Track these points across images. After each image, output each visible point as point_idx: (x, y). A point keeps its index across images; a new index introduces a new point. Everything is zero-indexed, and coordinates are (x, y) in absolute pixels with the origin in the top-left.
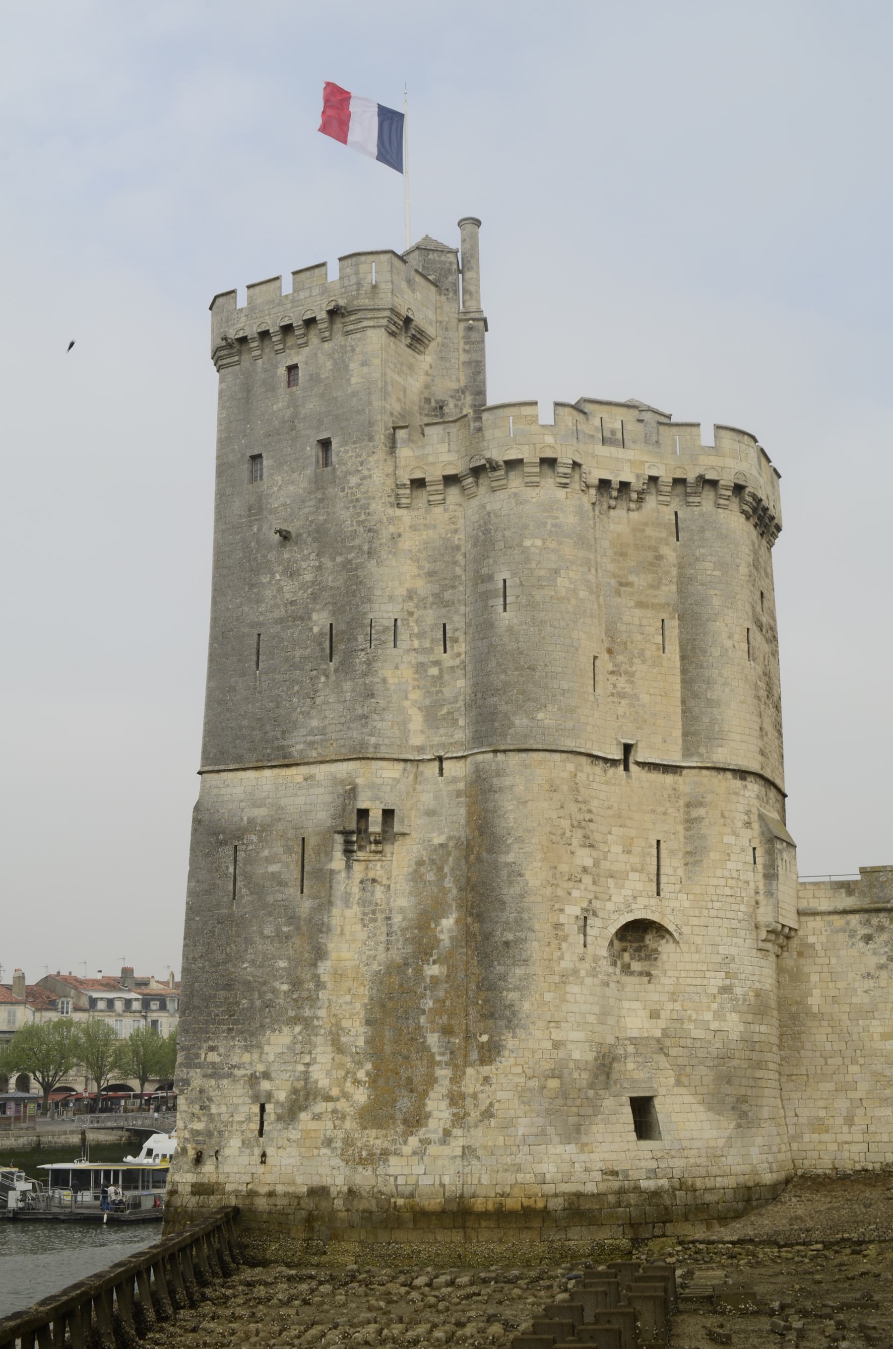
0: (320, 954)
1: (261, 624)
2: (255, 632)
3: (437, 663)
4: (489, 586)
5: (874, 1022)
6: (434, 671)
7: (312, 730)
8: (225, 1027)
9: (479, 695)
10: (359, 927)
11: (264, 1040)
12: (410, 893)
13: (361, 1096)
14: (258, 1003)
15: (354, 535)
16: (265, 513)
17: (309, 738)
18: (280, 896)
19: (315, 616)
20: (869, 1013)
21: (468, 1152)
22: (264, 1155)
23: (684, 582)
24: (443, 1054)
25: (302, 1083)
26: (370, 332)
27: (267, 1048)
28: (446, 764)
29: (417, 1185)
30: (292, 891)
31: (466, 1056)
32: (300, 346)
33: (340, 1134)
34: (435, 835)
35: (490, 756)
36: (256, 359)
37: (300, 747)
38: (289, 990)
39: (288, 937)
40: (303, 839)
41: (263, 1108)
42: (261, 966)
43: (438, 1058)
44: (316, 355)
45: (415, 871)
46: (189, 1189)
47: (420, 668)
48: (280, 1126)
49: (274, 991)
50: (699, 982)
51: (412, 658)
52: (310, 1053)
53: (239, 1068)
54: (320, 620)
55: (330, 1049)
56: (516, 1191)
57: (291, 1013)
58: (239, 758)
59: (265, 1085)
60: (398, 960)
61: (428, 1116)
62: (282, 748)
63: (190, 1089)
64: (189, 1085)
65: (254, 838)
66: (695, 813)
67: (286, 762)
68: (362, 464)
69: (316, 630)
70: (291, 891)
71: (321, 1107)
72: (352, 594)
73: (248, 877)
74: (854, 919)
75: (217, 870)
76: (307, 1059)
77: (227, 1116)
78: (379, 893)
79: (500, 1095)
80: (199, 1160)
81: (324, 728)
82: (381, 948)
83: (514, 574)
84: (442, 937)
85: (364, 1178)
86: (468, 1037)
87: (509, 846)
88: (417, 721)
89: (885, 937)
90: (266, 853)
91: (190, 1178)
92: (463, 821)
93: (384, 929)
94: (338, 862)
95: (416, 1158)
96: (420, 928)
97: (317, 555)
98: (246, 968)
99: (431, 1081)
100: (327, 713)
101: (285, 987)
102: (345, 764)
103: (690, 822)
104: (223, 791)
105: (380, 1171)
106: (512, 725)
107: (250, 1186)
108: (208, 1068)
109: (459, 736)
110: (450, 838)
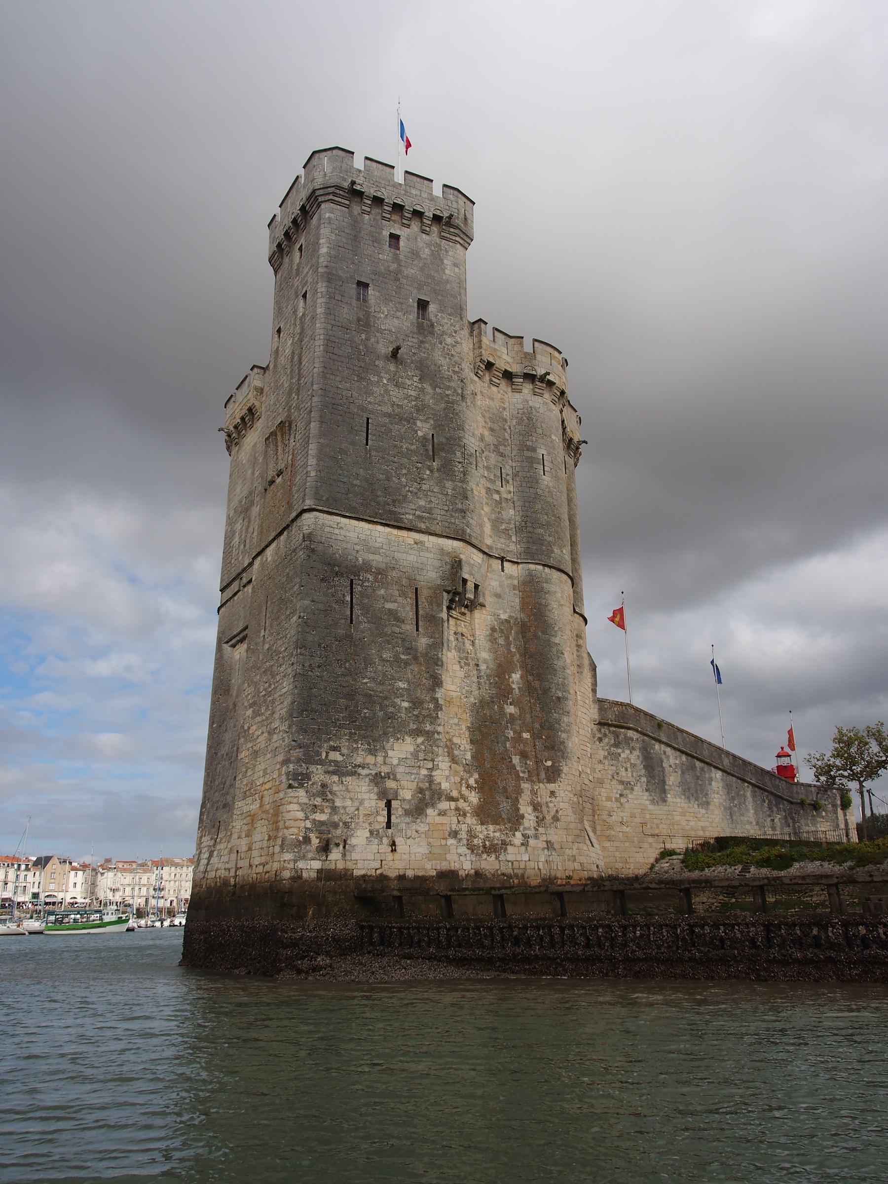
0: (436, 682)
1: (371, 412)
2: (365, 415)
3: (498, 492)
4: (533, 455)
5: (603, 790)
6: (496, 497)
7: (420, 507)
8: (347, 731)
9: (529, 524)
10: (457, 667)
11: (388, 746)
12: (490, 650)
13: (474, 798)
14: (381, 714)
15: (450, 379)
16: (373, 329)
17: (418, 513)
18: (397, 630)
19: (419, 423)
20: (601, 782)
21: (549, 845)
22: (393, 844)
24: (524, 772)
25: (427, 784)
26: (458, 246)
27: (390, 753)
28: (506, 564)
29: (525, 869)
30: (409, 627)
31: (538, 775)
32: (403, 225)
33: (464, 827)
34: (501, 612)
35: (541, 567)
36: (364, 212)
37: (411, 517)
38: (410, 707)
39: (407, 663)
40: (416, 589)
41: (388, 805)
42: (382, 683)
43: (521, 775)
44: (416, 239)
45: (491, 635)
46: (314, 875)
47: (488, 490)
48: (408, 820)
49: (394, 705)
50: (585, 748)
51: (483, 481)
52: (433, 760)
53: (363, 768)
54: (424, 428)
55: (447, 759)
56: (576, 877)
57: (413, 726)
58: (351, 509)
59: (391, 784)
60: (487, 697)
61: (523, 817)
62: (394, 513)
63: (310, 783)
64: (309, 779)
65: (371, 578)
66: (581, 642)
67: (399, 524)
68: (456, 332)
69: (420, 433)
70: (408, 627)
71: (444, 805)
72: (449, 421)
73: (366, 610)
75: (333, 596)
76: (430, 765)
77: (353, 809)
78: (468, 646)
79: (562, 805)
80: (325, 848)
81: (431, 509)
82: (475, 686)
83: (549, 454)
84: (514, 686)
85: (489, 864)
86: (538, 762)
87: (556, 632)
88: (488, 528)
89: (606, 740)
90: (382, 592)
91: (317, 865)
92: (518, 607)
93: (475, 672)
94: (444, 615)
95: (523, 848)
96: (499, 678)
97: (420, 379)
98: (367, 683)
99: (519, 791)
100: (433, 499)
101: (406, 704)
102: (450, 542)
104: (337, 531)
105: (502, 857)
106: (553, 552)
107: (378, 872)
108: (331, 765)
109: (512, 547)
110: (510, 617)
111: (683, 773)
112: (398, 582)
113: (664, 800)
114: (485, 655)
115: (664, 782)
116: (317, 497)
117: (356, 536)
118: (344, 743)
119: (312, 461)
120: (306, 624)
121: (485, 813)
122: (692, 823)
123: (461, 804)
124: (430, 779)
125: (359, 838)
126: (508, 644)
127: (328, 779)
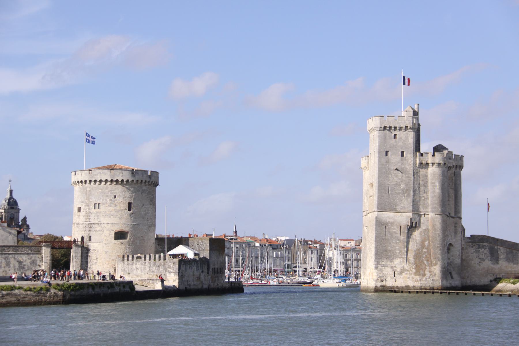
13: (414, 271)
21: (433, 280)
22: (396, 281)
23: (455, 184)
54: (403, 186)
58: (386, 210)
59: (395, 268)
71: (407, 272)
73: (389, 232)
74: (470, 244)
80: (382, 281)
91: (380, 284)
103: (455, 227)
111: (507, 254)
112: (396, 225)
113: (498, 263)
114: (418, 238)
115: (498, 258)
116: (378, 208)
117: (387, 216)
118: (385, 261)
119: (377, 200)
120: (376, 237)
121: (416, 274)
122: (510, 269)
123: (411, 272)
124: (404, 267)
125: (389, 279)
126: (425, 235)
127: (382, 268)
